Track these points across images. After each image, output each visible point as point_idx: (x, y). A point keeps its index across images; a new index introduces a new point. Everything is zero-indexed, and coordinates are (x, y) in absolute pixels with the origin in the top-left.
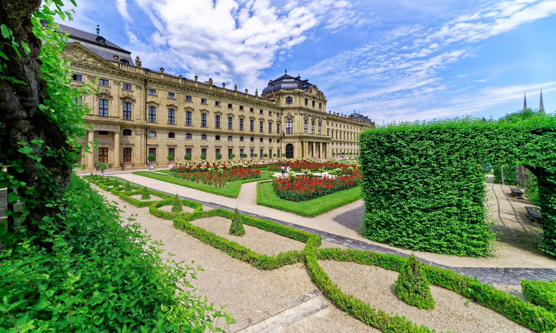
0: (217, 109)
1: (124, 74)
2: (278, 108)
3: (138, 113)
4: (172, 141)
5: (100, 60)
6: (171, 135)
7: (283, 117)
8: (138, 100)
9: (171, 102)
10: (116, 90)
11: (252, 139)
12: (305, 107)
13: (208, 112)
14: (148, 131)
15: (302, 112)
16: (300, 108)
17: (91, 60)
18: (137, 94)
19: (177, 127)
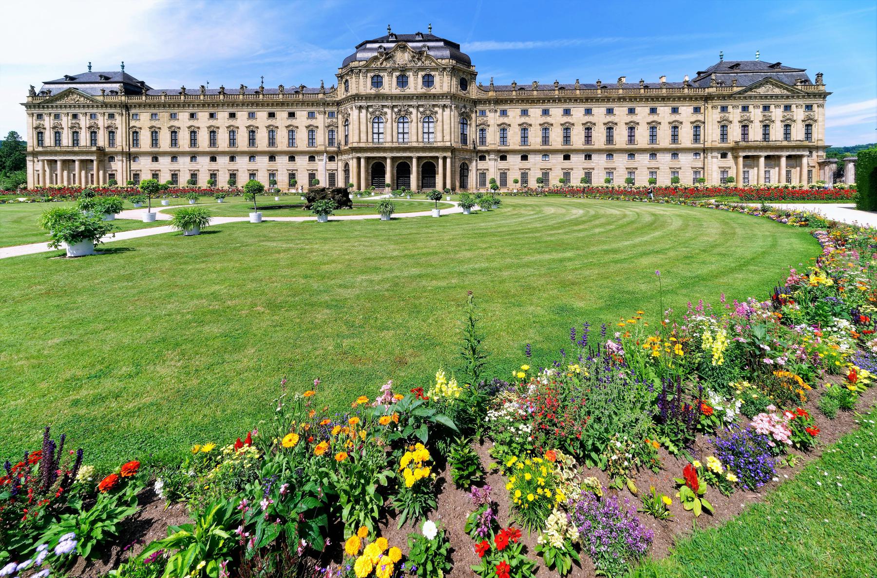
0: (212, 122)
1: (105, 105)
2: (326, 104)
3: (121, 141)
4: (155, 166)
5: (88, 99)
6: (155, 159)
7: (340, 116)
8: (120, 127)
9: (154, 123)
10: (102, 122)
11: (272, 158)
12: (373, 91)
13: (199, 128)
14: (131, 157)
15: (363, 103)
16: (357, 97)
17: (82, 99)
18: (119, 122)
19: (161, 150)
